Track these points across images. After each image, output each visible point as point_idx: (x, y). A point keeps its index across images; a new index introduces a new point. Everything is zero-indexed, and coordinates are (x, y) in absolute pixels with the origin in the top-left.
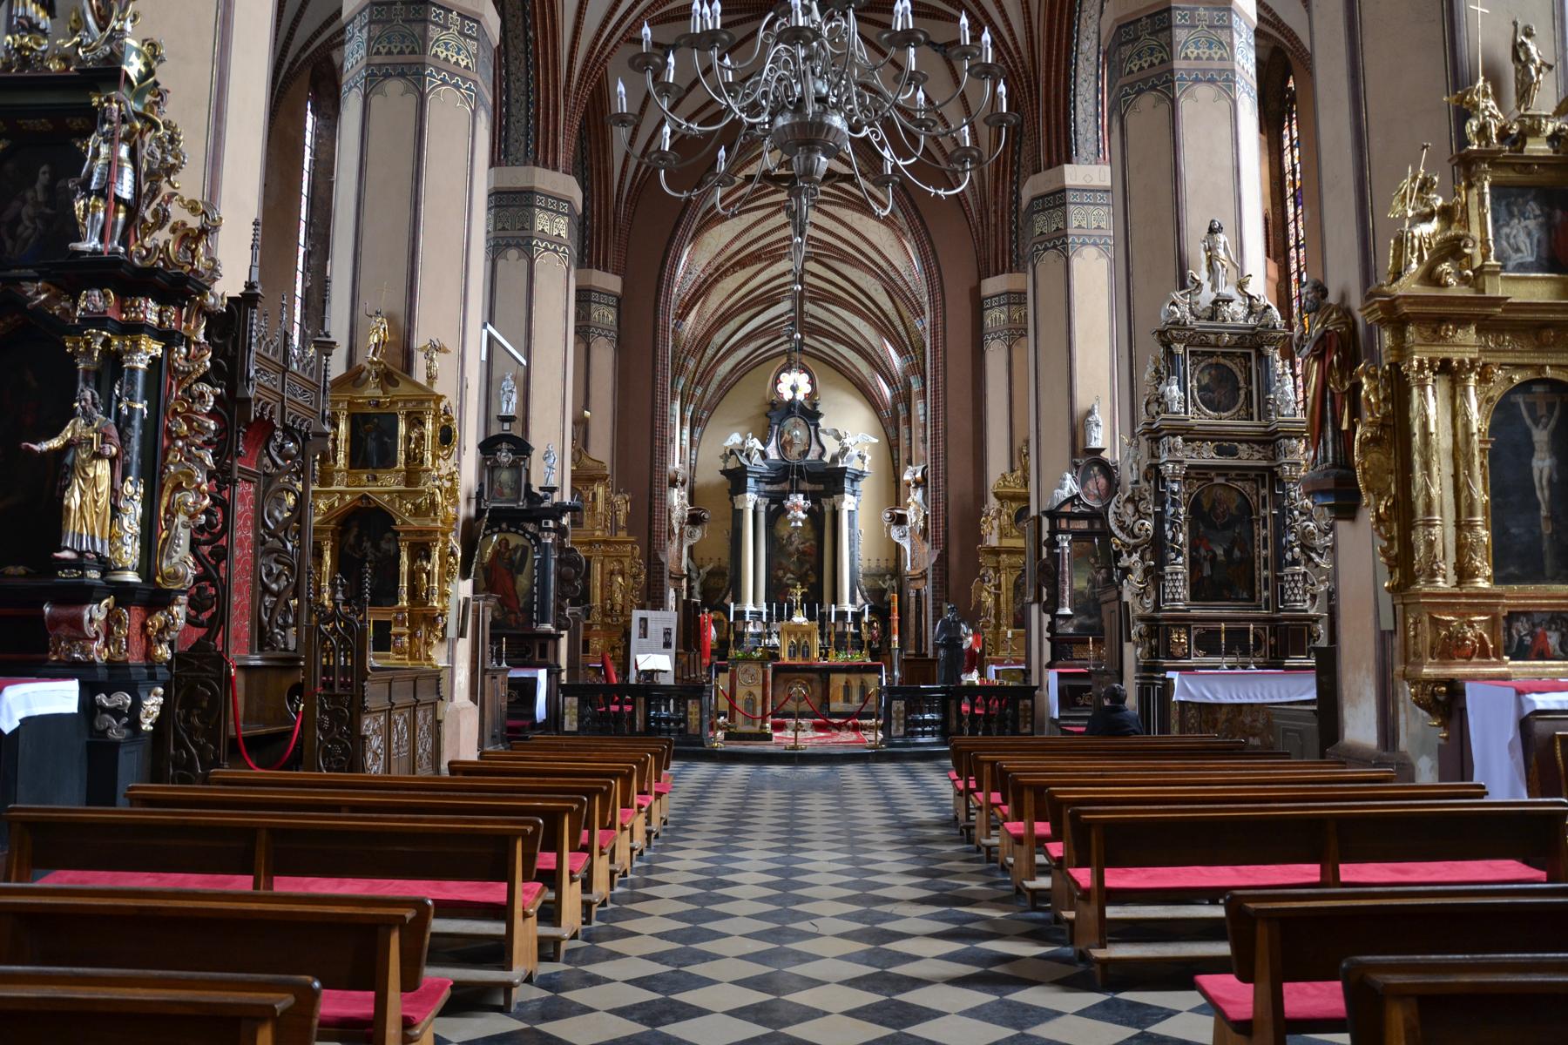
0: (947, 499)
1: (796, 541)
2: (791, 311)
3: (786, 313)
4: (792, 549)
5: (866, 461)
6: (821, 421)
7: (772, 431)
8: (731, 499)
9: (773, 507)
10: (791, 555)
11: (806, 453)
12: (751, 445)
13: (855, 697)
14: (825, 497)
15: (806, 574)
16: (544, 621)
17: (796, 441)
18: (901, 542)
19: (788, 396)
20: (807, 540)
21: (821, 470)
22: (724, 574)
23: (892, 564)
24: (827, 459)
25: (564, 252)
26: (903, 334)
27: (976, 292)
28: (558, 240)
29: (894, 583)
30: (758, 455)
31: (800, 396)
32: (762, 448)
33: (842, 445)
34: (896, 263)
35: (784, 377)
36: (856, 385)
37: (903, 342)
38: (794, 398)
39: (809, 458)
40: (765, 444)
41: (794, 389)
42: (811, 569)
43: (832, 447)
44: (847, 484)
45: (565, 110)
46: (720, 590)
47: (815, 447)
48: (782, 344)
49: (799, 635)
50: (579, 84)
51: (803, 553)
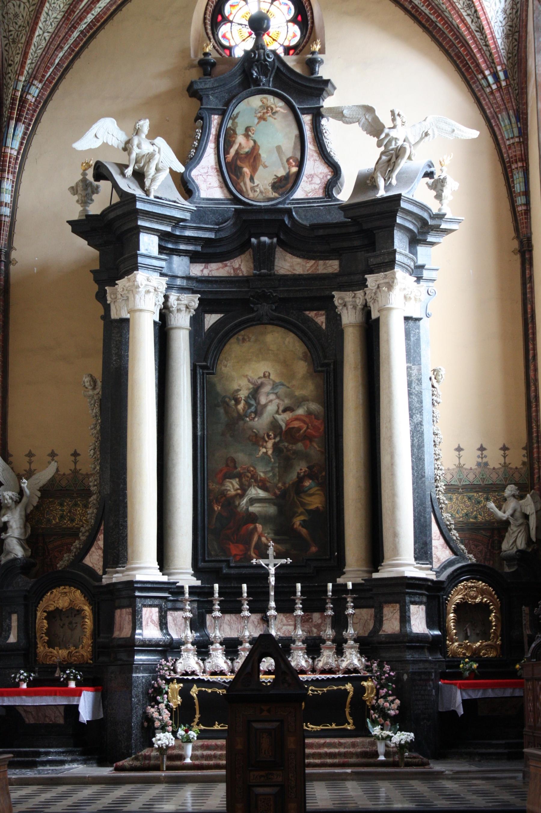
5: (447, 192)
6: (328, 103)
7: (205, 129)
8: (101, 297)
9: (211, 319)
12: (146, 148)
17: (264, 154)
20: (300, 401)
21: (339, 217)
22: (88, 493)
30: (165, 175)
32: (180, 168)
38: (259, 46)
39: (299, 194)
42: (311, 475)
46: (74, 534)
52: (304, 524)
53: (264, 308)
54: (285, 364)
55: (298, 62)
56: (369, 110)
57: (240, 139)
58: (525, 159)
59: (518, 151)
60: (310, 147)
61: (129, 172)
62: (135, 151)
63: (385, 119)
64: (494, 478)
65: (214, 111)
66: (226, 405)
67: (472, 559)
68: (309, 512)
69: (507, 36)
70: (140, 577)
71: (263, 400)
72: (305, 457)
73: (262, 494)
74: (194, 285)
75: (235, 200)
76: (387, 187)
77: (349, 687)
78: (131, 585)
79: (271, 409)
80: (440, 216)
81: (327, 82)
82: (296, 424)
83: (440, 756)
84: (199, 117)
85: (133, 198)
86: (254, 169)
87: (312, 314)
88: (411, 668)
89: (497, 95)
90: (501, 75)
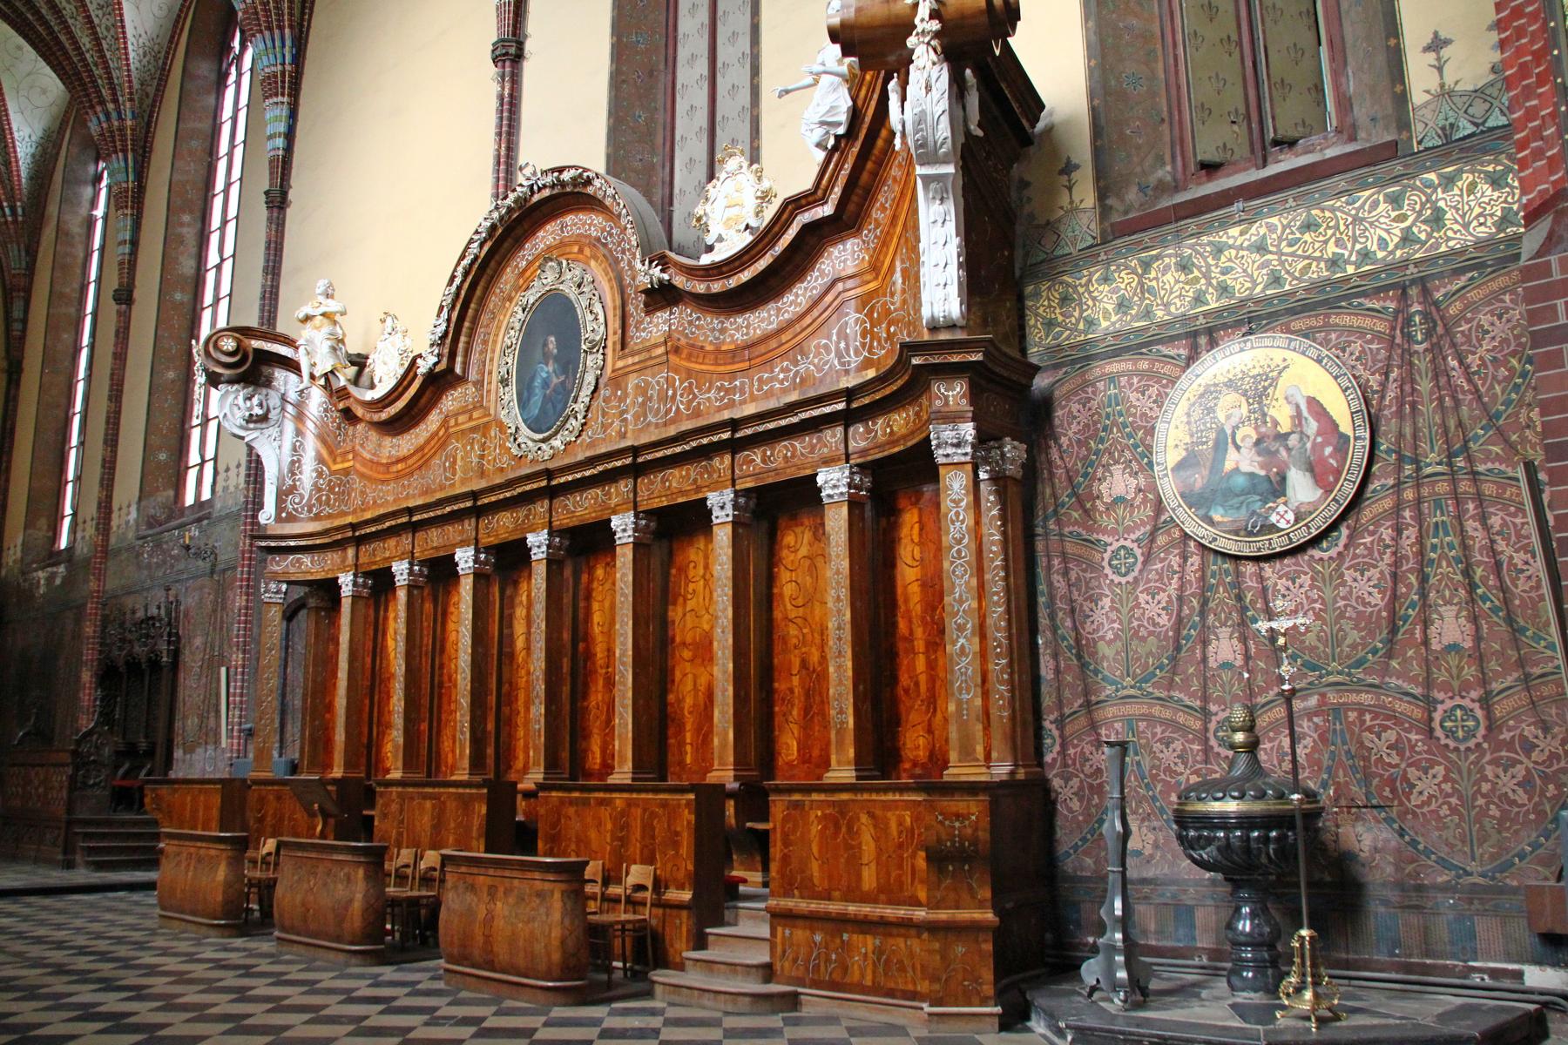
58: (28, 291)
69: (31, 178)
89: (11, 227)
90: (20, 211)
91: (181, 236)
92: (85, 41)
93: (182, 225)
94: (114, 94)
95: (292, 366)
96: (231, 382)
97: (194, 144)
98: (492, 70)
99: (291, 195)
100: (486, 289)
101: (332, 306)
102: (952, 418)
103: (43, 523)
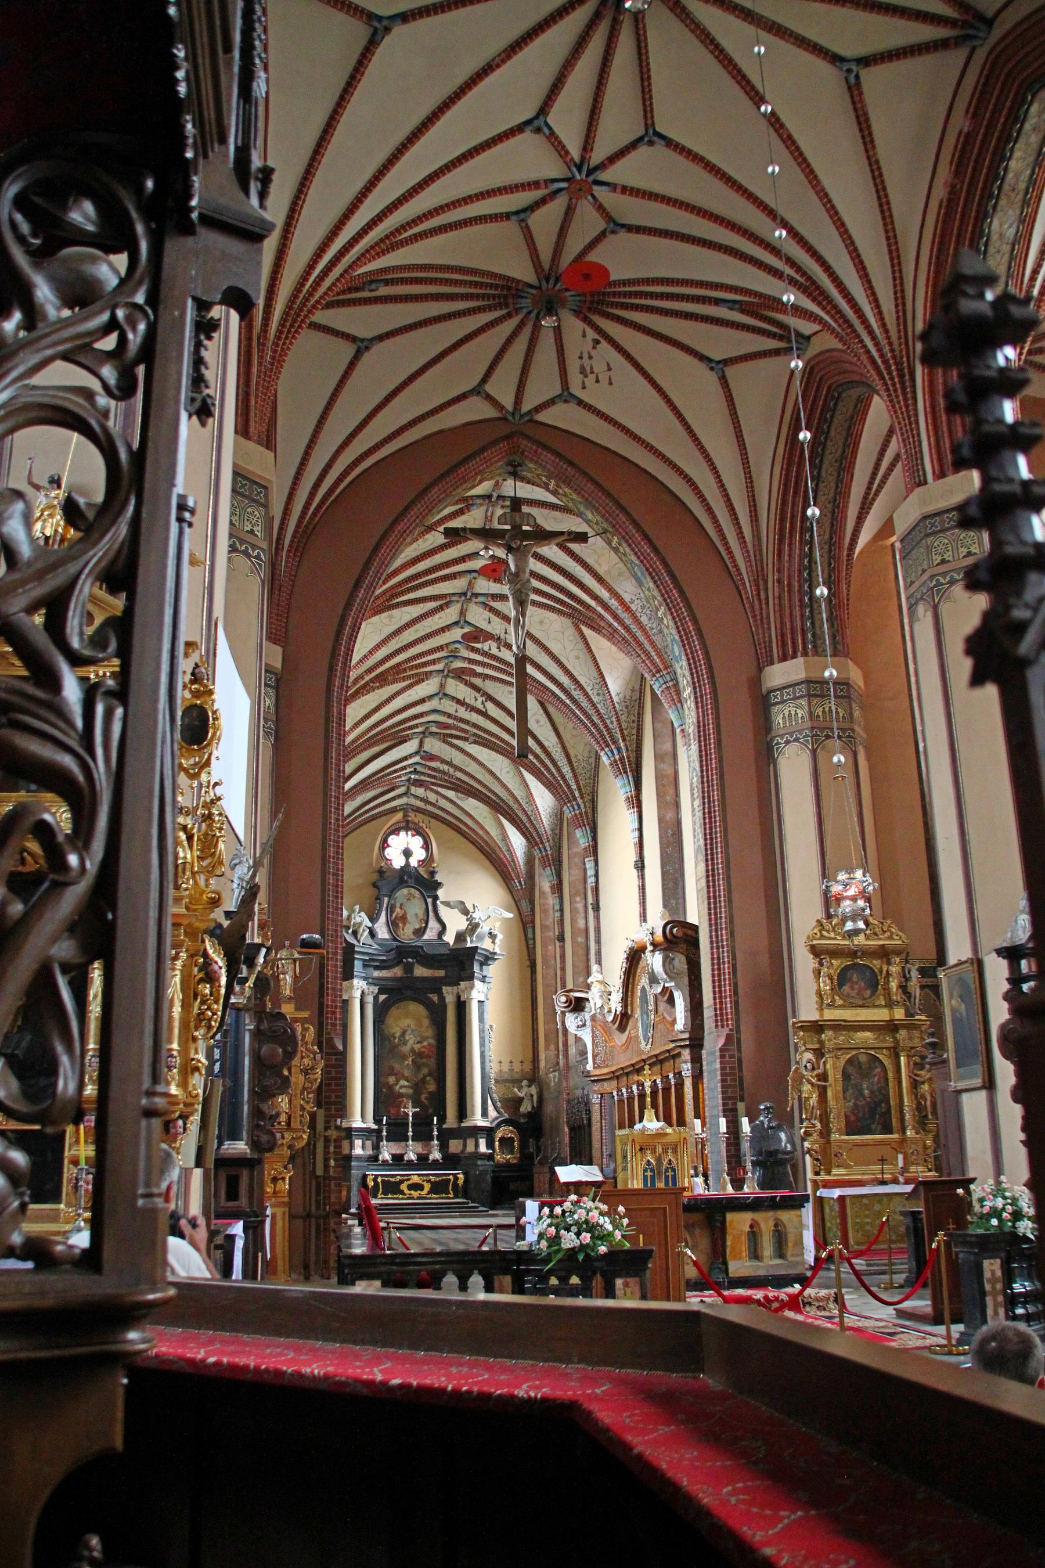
0: (734, 958)
1: (411, 1040)
2: (417, 753)
3: (411, 756)
4: (406, 1049)
5: (497, 941)
6: (440, 893)
7: (381, 905)
9: (382, 997)
10: (404, 1057)
11: (420, 932)
12: (358, 920)
13: (767, 1249)
14: (447, 984)
15: (423, 1081)
16: (235, 1136)
17: (409, 917)
18: (579, 1034)
19: (398, 862)
20: (425, 1039)
23: (528, 1067)
24: (450, 938)
25: (258, 557)
26: (569, 776)
27: (756, 681)
28: (250, 538)
29: (533, 1090)
31: (414, 862)
32: (370, 925)
33: (470, 920)
34: (582, 680)
35: (392, 840)
36: (481, 850)
37: (569, 786)
38: (407, 864)
39: (426, 937)
40: (373, 919)
41: (407, 853)
42: (430, 1074)
43: (455, 923)
44: (476, 968)
45: (260, 364)
47: (433, 925)
48: (393, 799)
49: (660, 1150)
50: (280, 332)
51: (420, 1054)
52: (426, 1098)
53: (409, 992)
54: (418, 1020)
55: (426, 871)
56: (463, 903)
57: (398, 910)
58: (533, 922)
59: (529, 919)
60: (431, 914)
61: (350, 931)
62: (353, 921)
63: (471, 909)
64: (516, 1076)
65: (386, 896)
66: (390, 1041)
67: (506, 1116)
68: (430, 1093)
70: (354, 1126)
71: (407, 1038)
72: (427, 1066)
73: (406, 1083)
74: (376, 982)
75: (395, 940)
76: (472, 941)
77: (451, 1177)
78: (349, 1131)
79: (411, 1042)
80: (495, 953)
81: (440, 884)
82: (423, 1050)
83: (493, 1209)
84: (377, 898)
85: (354, 945)
86: (404, 924)
87: (431, 996)
88: (481, 1168)
91: (576, 908)
92: (524, 819)
93: (576, 902)
94: (541, 840)
95: (588, 1000)
96: (570, 1011)
97: (577, 860)
98: (635, 871)
99: (601, 904)
100: (634, 980)
101: (600, 977)
102: (685, 1062)
103: (552, 1047)
